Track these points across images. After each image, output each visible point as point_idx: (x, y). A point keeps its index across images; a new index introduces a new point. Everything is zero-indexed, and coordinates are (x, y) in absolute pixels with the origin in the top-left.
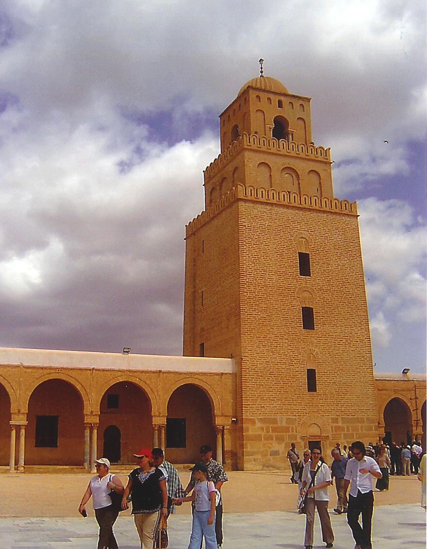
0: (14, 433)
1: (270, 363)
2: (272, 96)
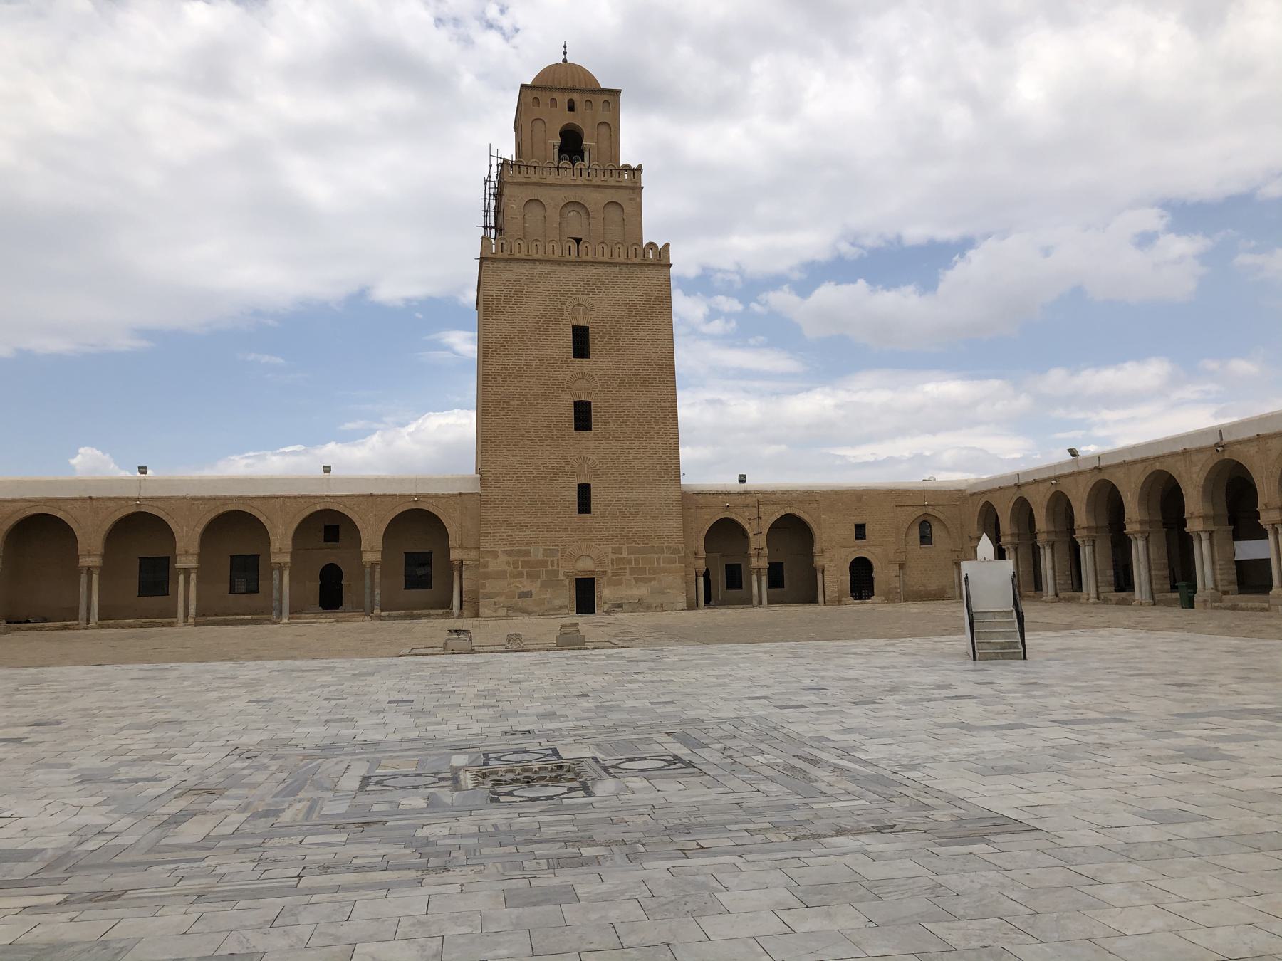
0: (181, 578)
2: (556, 95)
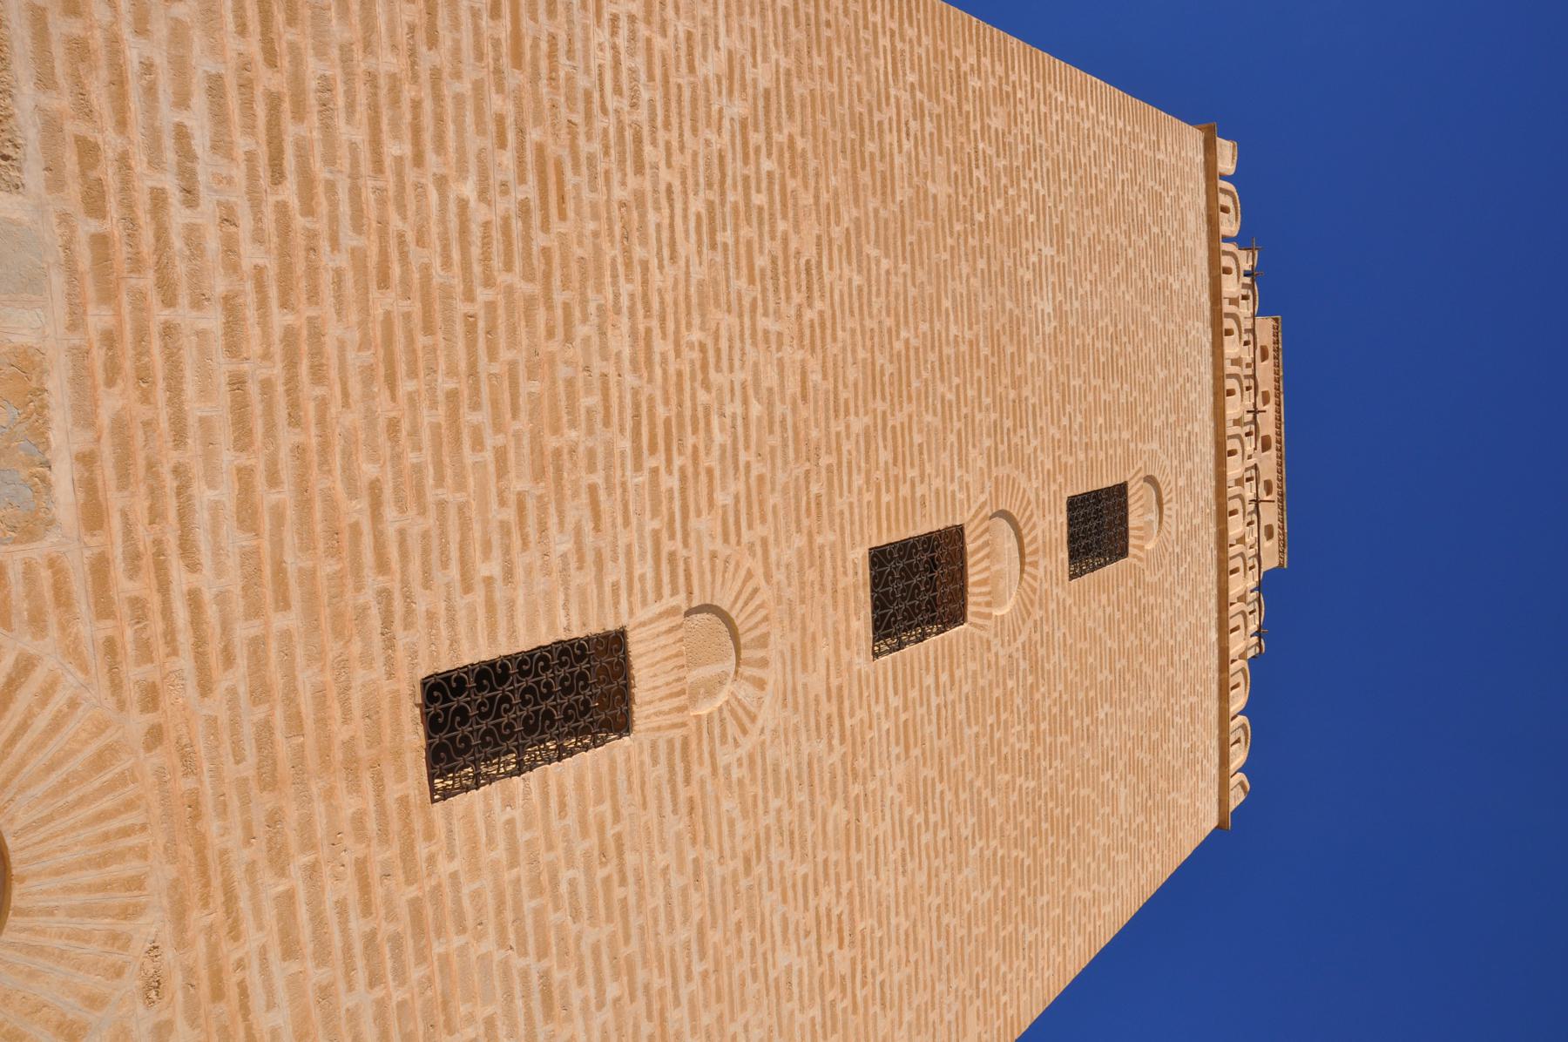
1: (632, 181)
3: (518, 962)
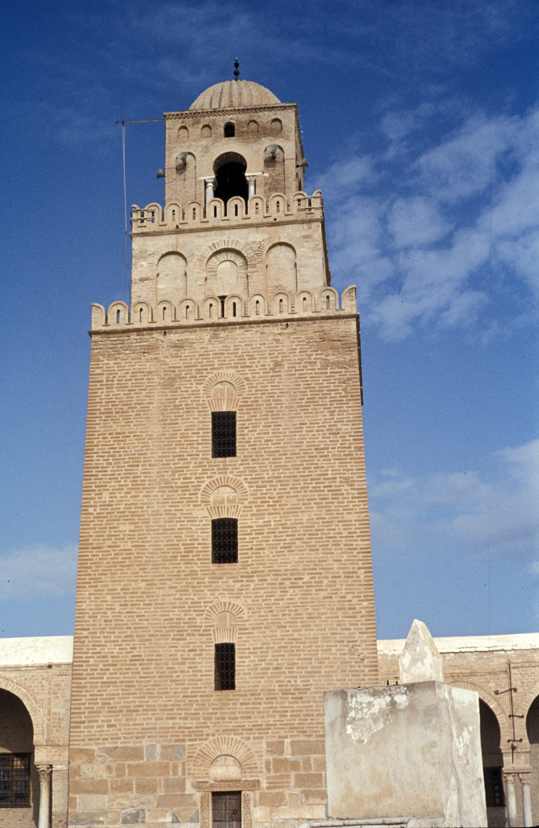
3: (269, 675)
